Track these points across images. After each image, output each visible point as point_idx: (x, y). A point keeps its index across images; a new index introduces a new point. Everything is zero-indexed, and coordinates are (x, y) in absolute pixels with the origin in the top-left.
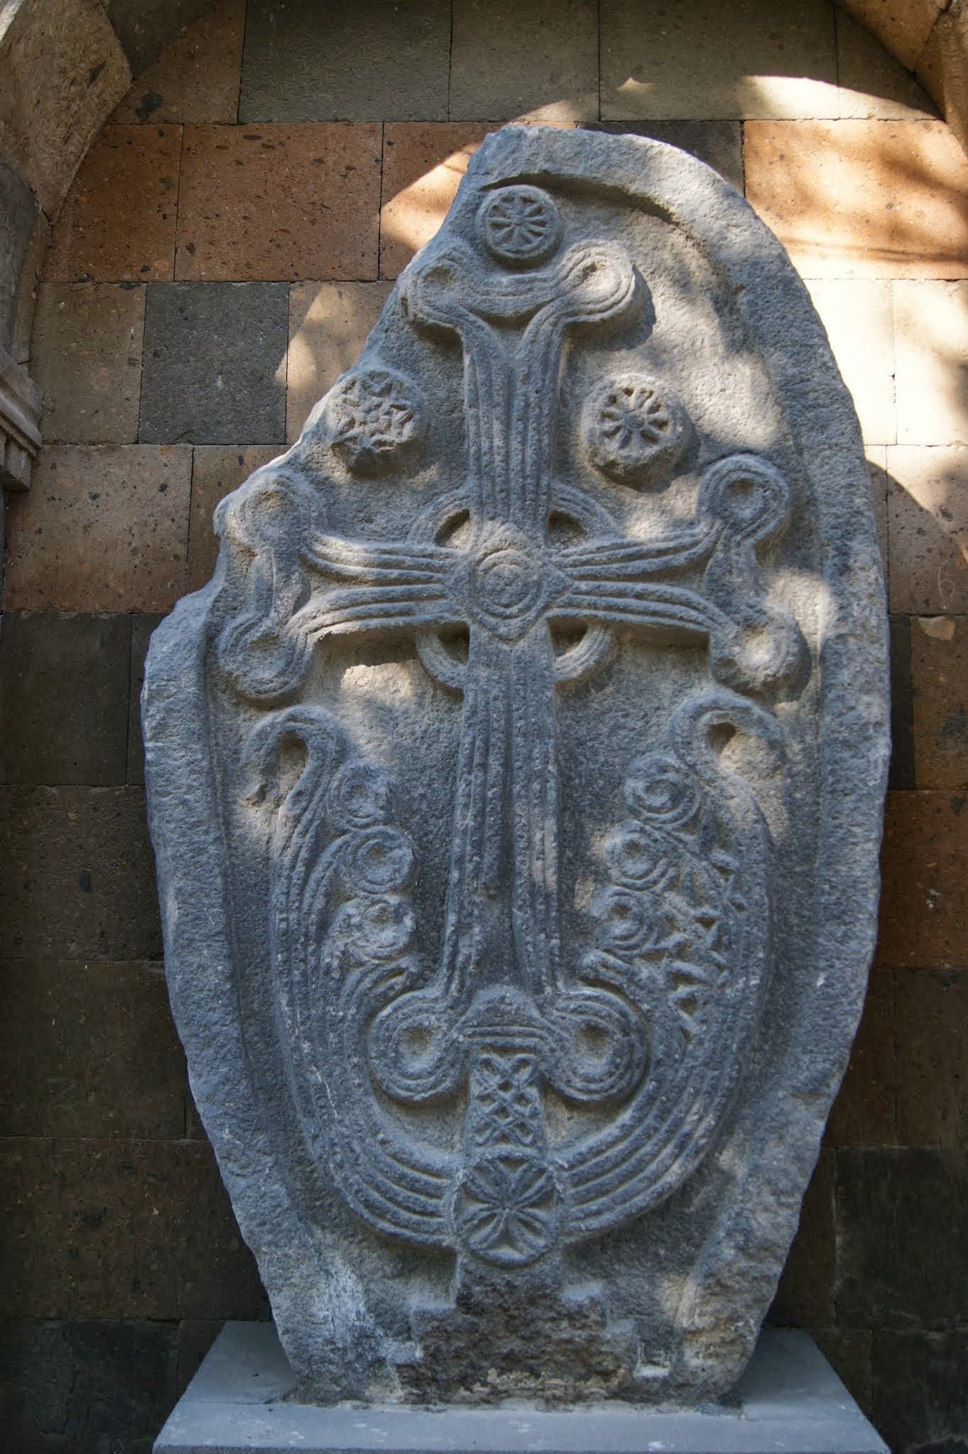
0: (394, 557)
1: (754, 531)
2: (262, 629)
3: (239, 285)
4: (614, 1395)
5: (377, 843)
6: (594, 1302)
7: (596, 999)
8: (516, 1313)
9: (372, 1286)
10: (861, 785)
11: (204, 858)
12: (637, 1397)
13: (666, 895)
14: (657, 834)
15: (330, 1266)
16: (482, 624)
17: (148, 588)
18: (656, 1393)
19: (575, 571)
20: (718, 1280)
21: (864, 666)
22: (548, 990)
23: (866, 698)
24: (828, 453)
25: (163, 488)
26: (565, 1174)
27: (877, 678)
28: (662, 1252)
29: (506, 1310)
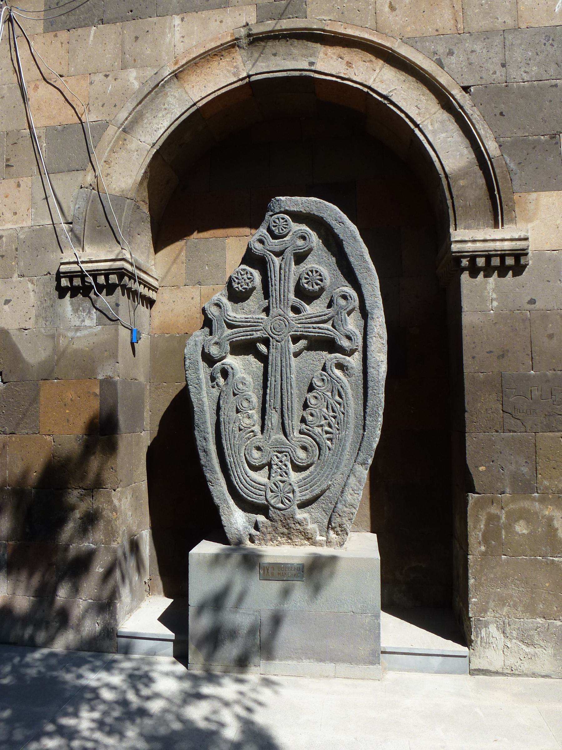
4: (312, 545)
6: (305, 519)
8: (284, 522)
11: (201, 402)
14: (320, 393)
16: (272, 338)
19: (297, 322)
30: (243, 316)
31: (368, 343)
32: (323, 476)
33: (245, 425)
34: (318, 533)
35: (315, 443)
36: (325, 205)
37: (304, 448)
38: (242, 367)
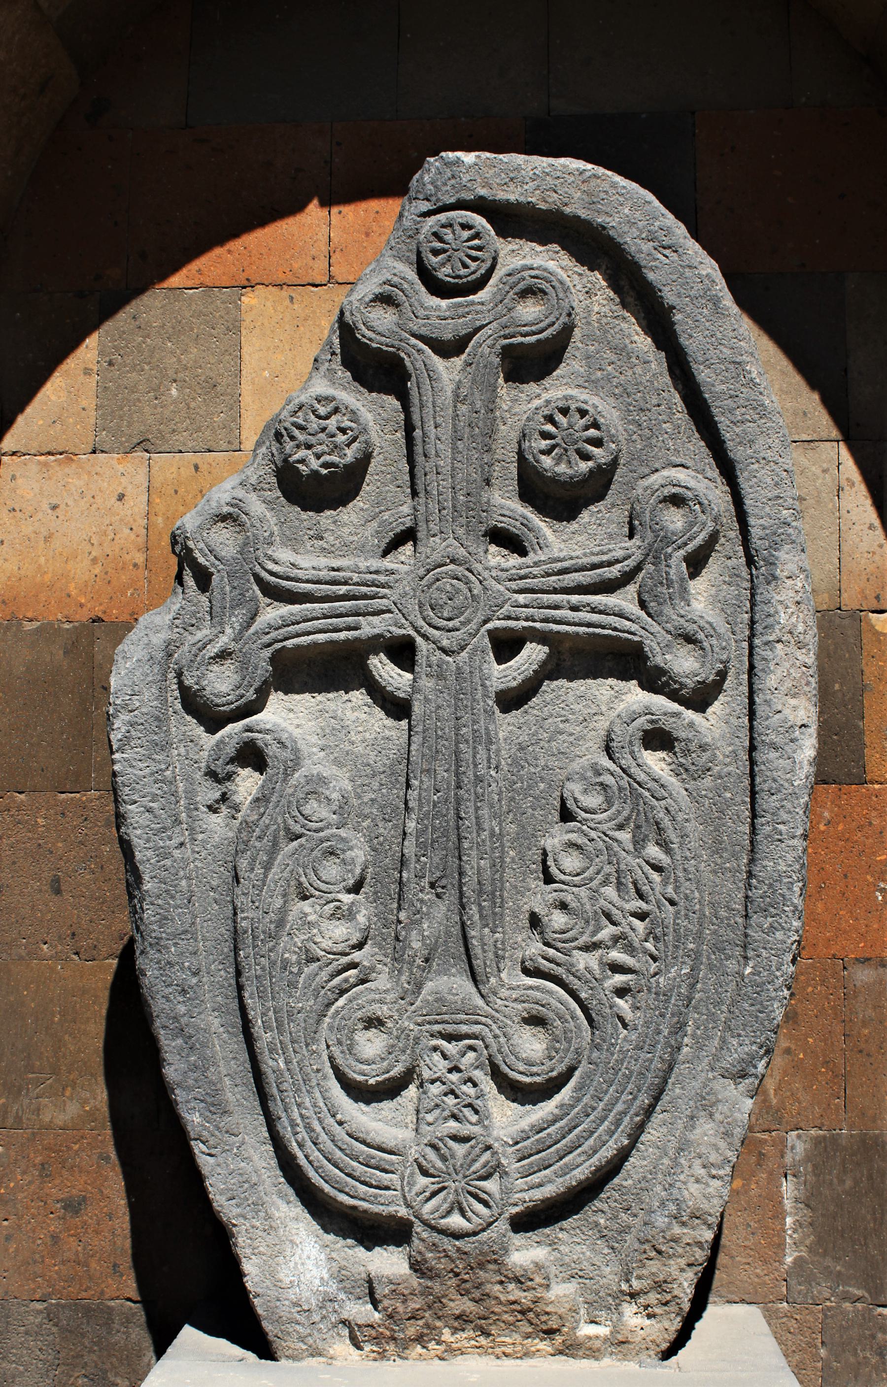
0: (341, 574)
1: (686, 544)
2: (218, 645)
3: (191, 291)
4: (561, 1353)
5: (331, 846)
6: (538, 1266)
7: (537, 988)
8: (466, 1277)
9: (334, 1255)
10: (786, 785)
11: (168, 862)
12: (580, 1353)
13: (603, 890)
14: (593, 834)
15: (296, 1237)
16: (425, 637)
17: (109, 597)
18: (599, 1350)
19: (514, 585)
20: (653, 1246)
21: (792, 671)
22: (493, 980)
23: (793, 702)
24: (756, 466)
25: (121, 497)
26: (510, 1150)
27: (804, 682)
28: (602, 1221)
29: (457, 1275)
30: (323, 562)
31: (759, 665)
32: (603, 1119)
33: (326, 944)
34: (582, 1311)
35: (574, 1005)
36: (614, 185)
37: (536, 1021)
38: (314, 739)
